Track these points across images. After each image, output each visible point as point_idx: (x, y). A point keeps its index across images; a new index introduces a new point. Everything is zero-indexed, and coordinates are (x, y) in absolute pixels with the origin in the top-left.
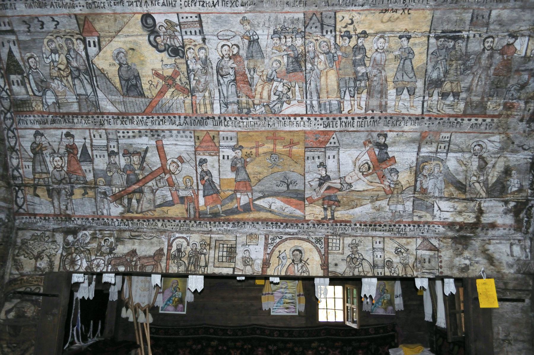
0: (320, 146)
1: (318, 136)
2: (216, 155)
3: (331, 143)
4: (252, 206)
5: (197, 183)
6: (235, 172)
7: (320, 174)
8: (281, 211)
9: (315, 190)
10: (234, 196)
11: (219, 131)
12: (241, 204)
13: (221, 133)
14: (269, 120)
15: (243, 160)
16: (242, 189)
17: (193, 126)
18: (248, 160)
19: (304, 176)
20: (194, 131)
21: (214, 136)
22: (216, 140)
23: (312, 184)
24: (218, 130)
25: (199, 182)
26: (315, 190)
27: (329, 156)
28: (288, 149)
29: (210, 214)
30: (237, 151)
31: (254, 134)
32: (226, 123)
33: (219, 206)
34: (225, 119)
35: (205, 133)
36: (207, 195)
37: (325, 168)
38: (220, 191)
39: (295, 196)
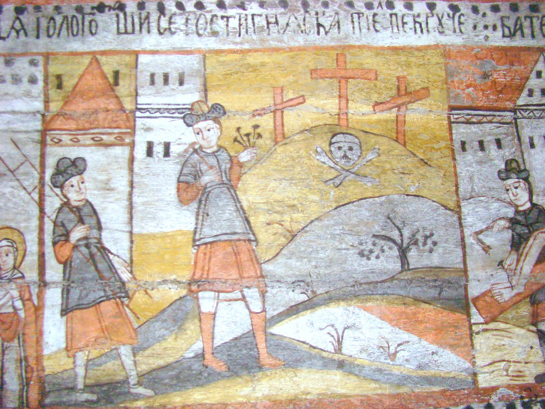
0: (500, 105)
1: (488, 68)
2: (120, 142)
3: (531, 93)
4: (262, 346)
5: (42, 256)
6: (195, 205)
7: (511, 203)
8: (383, 361)
9: (501, 263)
10: (189, 305)
11: (136, 54)
12: (218, 342)
13: (143, 59)
14: (320, 9)
15: (223, 156)
16: (224, 275)
17: (44, 39)
18: (245, 157)
19: (458, 211)
20: (47, 56)
21: (116, 74)
22: (123, 89)
23: (489, 240)
24: (135, 47)
25: (49, 250)
26: (501, 263)
27: (531, 139)
28: (392, 115)
29: (88, 388)
30: (202, 125)
31: (266, 59)
32: (164, 24)
33: (125, 351)
34: (161, 9)
35: (86, 60)
36: (79, 307)
37: (526, 179)
38: (131, 286)
39: (434, 293)
